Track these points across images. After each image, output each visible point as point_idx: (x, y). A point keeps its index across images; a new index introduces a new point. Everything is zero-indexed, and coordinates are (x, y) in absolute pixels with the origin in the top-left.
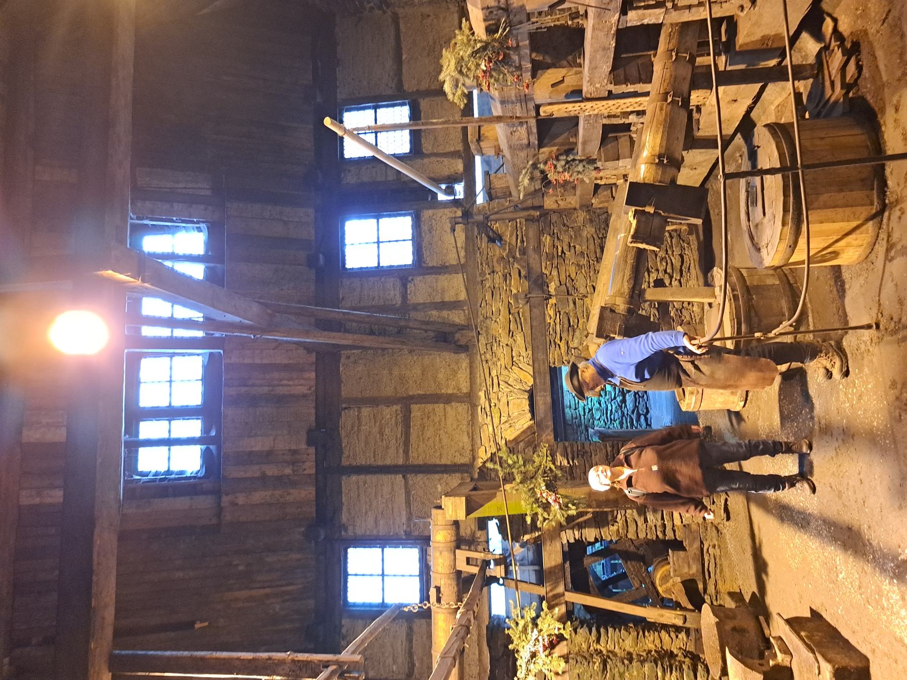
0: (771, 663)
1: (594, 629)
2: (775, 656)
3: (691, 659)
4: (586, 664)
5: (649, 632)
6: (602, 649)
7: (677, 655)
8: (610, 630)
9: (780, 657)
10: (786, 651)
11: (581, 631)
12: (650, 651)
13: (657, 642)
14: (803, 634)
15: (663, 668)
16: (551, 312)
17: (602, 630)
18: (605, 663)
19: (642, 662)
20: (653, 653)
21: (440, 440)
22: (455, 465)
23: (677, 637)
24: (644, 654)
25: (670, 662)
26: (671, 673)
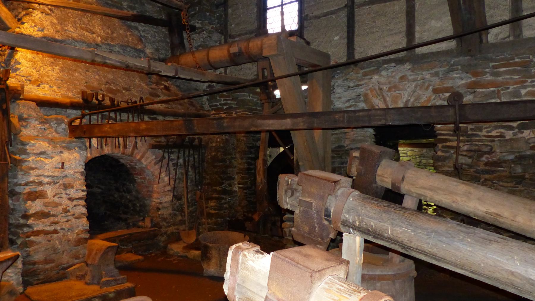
16: (494, 133)
21: (373, 33)
22: (353, 49)
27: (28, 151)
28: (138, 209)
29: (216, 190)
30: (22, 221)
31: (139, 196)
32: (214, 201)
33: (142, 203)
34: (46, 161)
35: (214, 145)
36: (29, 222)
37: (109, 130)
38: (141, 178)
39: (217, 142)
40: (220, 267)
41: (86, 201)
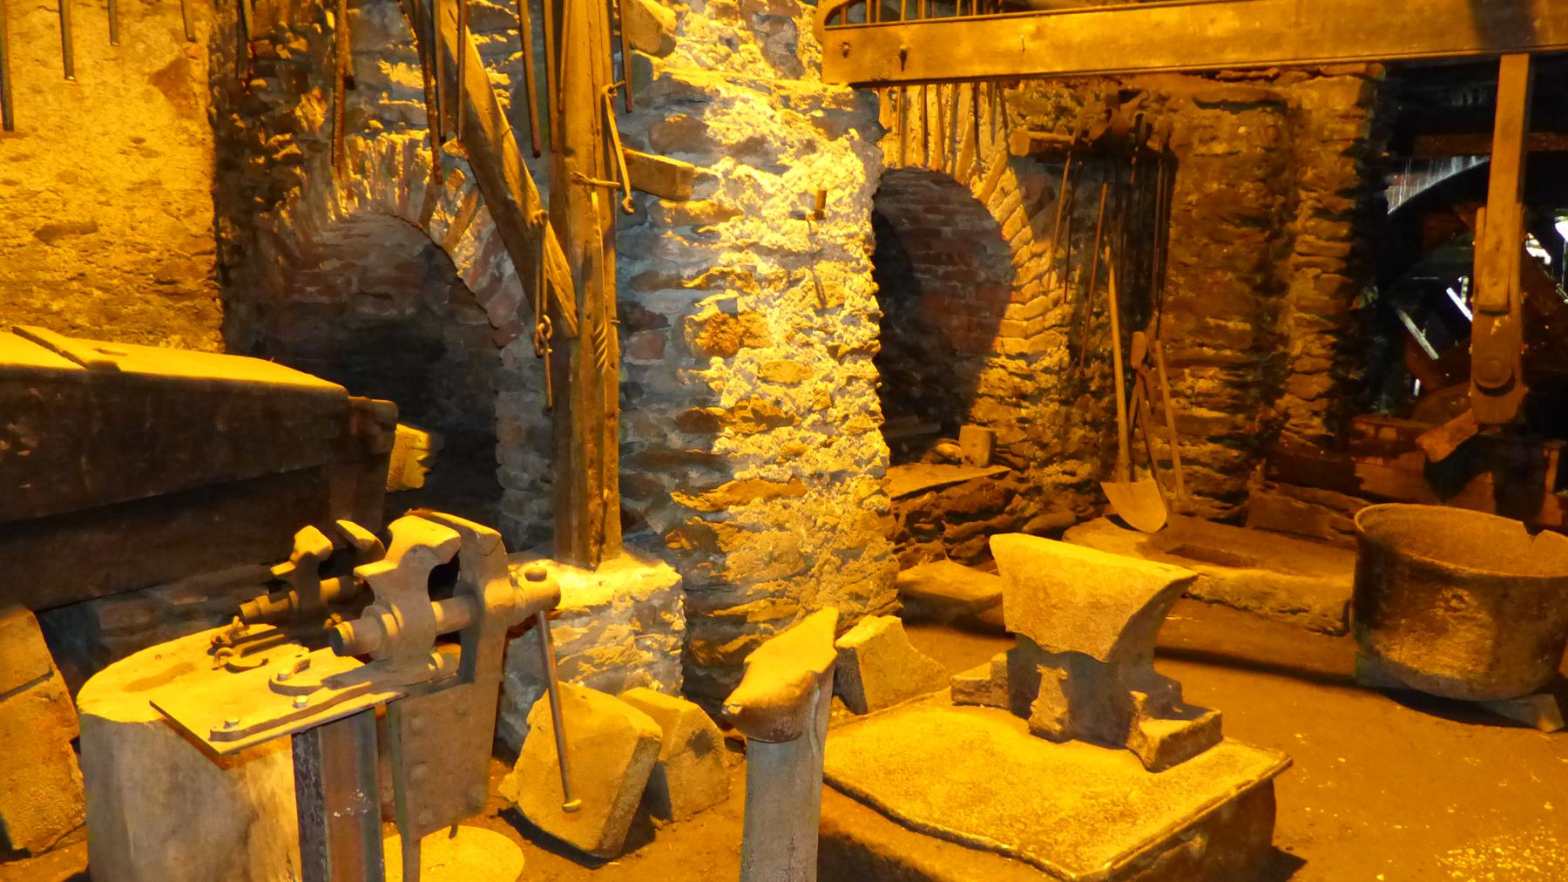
0: (1140, 696)
2: (1165, 713)
3: (1258, 436)
4: (1258, 173)
5: (1333, 345)
6: (1298, 225)
7: (1271, 404)
8: (1345, 247)
9: (1157, 729)
10: (1170, 753)
11: (1349, 169)
13: (1307, 364)
14: (1197, 843)
18: (1259, 220)
19: (1256, 318)
20: (1281, 349)
23: (1316, 414)
27: (710, 133)
28: (916, 392)
29: (1222, 331)
30: (676, 440)
31: (926, 343)
32: (1212, 372)
33: (935, 371)
34: (766, 179)
35: (1219, 148)
36: (719, 446)
37: (1031, 45)
38: (947, 277)
39: (1234, 137)
40: (1491, 667)
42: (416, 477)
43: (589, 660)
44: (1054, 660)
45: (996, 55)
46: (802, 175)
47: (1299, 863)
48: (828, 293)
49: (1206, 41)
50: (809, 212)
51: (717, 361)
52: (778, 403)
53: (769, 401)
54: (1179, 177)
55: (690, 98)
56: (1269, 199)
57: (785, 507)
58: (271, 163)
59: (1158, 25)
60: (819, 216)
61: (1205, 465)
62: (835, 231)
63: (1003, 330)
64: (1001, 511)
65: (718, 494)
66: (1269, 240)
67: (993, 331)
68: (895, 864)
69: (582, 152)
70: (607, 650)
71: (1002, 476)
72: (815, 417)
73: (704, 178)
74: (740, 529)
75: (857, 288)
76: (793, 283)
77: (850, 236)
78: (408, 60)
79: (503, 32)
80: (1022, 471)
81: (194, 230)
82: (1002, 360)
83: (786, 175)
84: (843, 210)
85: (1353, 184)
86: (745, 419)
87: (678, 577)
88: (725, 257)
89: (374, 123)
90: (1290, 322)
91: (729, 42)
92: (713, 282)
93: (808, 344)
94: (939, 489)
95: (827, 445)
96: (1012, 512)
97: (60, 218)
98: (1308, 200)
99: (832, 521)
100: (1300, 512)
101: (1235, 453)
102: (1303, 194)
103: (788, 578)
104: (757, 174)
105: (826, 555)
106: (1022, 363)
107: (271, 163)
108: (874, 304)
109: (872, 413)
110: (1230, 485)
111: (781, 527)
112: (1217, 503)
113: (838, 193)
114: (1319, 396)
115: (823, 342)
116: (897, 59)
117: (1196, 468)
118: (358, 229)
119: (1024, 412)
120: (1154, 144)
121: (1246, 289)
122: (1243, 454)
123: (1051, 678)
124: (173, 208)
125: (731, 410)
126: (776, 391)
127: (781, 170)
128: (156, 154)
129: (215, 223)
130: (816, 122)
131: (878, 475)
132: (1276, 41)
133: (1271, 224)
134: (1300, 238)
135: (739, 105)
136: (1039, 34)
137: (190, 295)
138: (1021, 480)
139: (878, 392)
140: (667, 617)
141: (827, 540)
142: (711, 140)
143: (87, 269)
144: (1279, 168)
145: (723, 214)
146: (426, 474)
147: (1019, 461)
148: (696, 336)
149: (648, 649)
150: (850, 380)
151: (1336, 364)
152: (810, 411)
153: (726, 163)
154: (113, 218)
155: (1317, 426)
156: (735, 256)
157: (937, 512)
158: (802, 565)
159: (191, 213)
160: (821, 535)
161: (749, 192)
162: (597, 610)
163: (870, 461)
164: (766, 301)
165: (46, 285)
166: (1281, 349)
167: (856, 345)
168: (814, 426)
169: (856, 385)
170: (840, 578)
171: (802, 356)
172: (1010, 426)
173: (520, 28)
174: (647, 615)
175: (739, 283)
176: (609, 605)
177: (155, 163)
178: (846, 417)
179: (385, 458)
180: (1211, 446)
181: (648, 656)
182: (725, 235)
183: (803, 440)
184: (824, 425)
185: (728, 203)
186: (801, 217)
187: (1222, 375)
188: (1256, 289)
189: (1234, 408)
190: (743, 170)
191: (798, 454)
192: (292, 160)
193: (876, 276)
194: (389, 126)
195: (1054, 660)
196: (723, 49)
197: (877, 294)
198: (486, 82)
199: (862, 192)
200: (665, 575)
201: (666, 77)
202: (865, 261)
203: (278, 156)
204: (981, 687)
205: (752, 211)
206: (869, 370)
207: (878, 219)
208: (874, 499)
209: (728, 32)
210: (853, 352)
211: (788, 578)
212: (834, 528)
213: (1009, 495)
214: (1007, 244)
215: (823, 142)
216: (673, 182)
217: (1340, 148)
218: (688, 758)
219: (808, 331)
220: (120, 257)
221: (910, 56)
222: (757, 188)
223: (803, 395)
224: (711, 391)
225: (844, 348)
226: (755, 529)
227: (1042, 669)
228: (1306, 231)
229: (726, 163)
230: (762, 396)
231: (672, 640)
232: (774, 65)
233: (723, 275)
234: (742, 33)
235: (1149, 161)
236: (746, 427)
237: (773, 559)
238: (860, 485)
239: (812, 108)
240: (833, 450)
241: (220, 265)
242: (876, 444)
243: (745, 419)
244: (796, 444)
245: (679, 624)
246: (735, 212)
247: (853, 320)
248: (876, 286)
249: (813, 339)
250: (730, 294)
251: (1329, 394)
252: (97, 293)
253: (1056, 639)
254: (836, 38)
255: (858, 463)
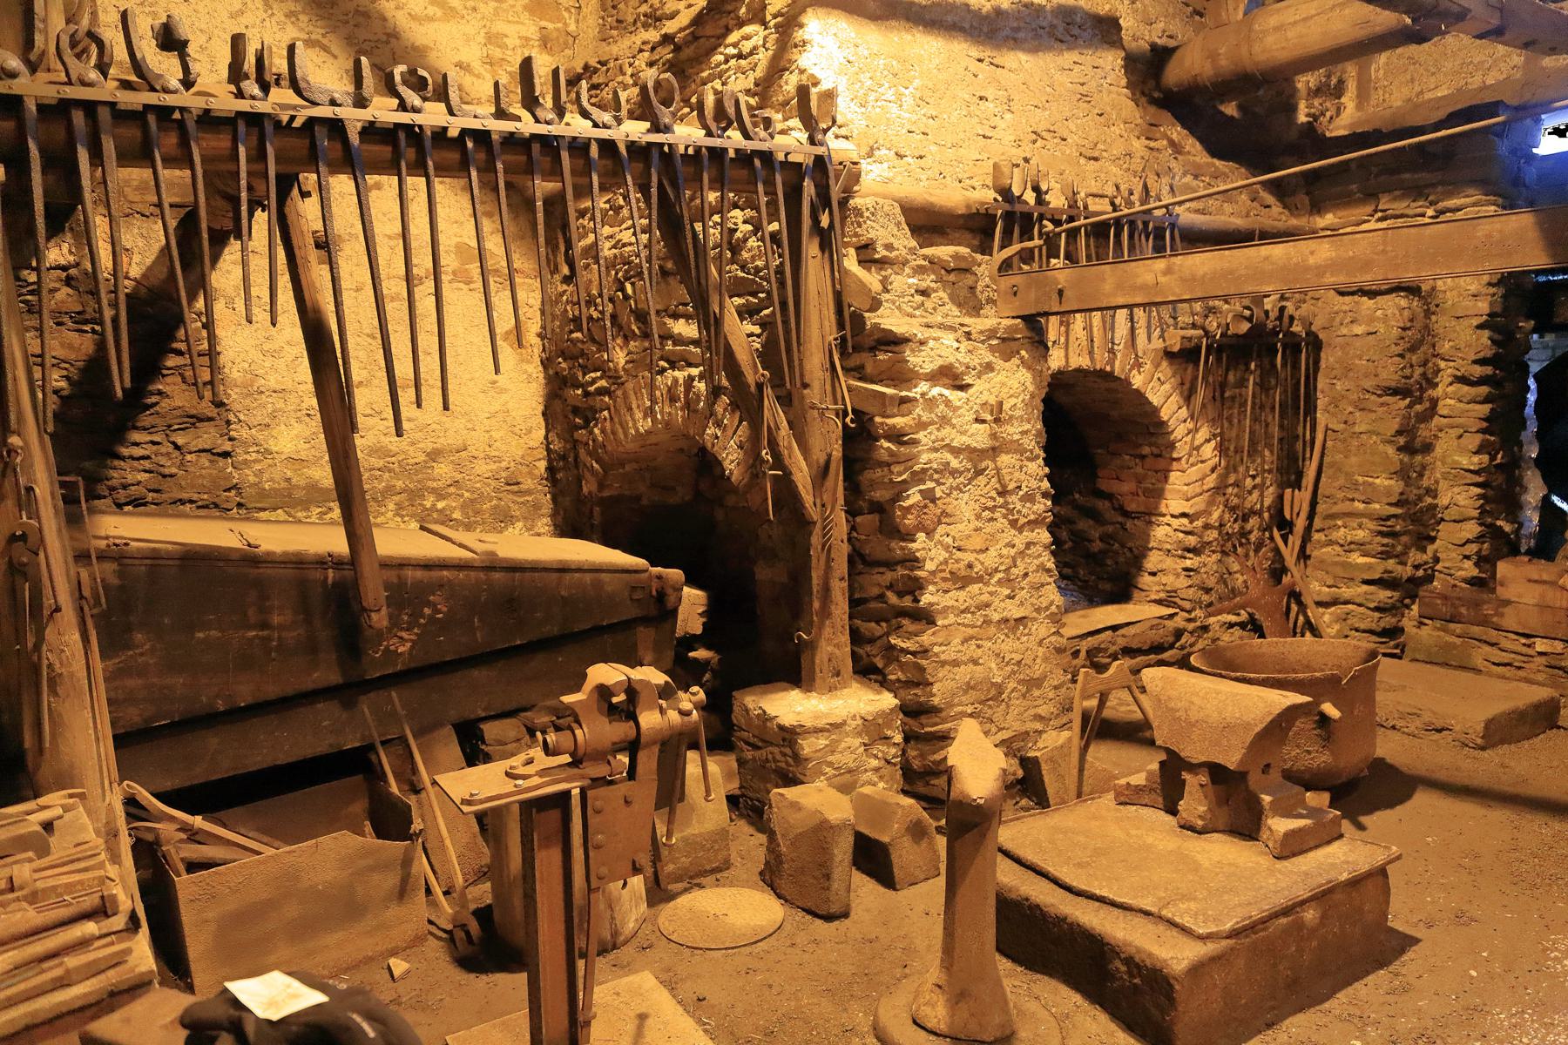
0: (1267, 798)
1: (1489, 370)
4: (1398, 350)
5: (1480, 496)
7: (1424, 550)
9: (1280, 825)
10: (1291, 847)
12: (1433, 492)
13: (1453, 513)
14: (1310, 915)
15: (1388, 518)
17: (1484, 390)
19: (1402, 473)
20: (1429, 500)
23: (1467, 557)
24: (1425, 483)
25: (1405, 533)
26: (1381, 533)
33: (1110, 529)
34: (955, 396)
37: (1162, 279)
41: (1052, 529)
42: (696, 627)
43: (830, 764)
44: (1193, 768)
45: (1135, 289)
46: (983, 390)
47: (1416, 941)
48: (1007, 478)
49: (1307, 269)
50: (989, 418)
51: (921, 536)
52: (970, 566)
53: (962, 565)
54: (1323, 355)
55: (893, 342)
56: (1408, 372)
57: (979, 647)
58: (587, 394)
59: (1267, 258)
60: (997, 420)
61: (1360, 605)
62: (1011, 430)
63: (1167, 495)
64: (1172, 646)
65: (926, 639)
66: (1410, 406)
67: (1158, 494)
68: (1061, 920)
69: (816, 385)
70: (844, 759)
71: (1171, 616)
72: (1001, 575)
73: (904, 401)
74: (943, 663)
75: (1032, 473)
76: (979, 473)
77: (1023, 433)
78: (688, 317)
79: (754, 294)
80: (1189, 612)
81: (532, 444)
82: (1168, 519)
83: (971, 391)
84: (1018, 413)
85: (1489, 353)
86: (944, 580)
87: (897, 701)
88: (924, 458)
89: (662, 363)
90: (1436, 473)
91: (924, 293)
92: (919, 477)
93: (992, 519)
94: (1115, 628)
95: (1011, 597)
96: (1182, 648)
97: (442, 442)
98: (1447, 371)
99: (1017, 657)
100: (1454, 646)
101: (1389, 593)
102: (1442, 364)
103: (982, 702)
104: (946, 392)
105: (1012, 685)
106: (1185, 521)
107: (587, 394)
108: (1046, 484)
109: (1048, 571)
110: (1388, 621)
111: (975, 662)
112: (1374, 638)
113: (1013, 401)
114: (1468, 541)
115: (1005, 516)
116: (1055, 296)
117: (1350, 606)
118: (653, 439)
119: (1188, 563)
120: (1297, 328)
121: (1391, 450)
122: (1396, 595)
123: (1192, 781)
124: (516, 430)
125: (933, 573)
126: (968, 557)
127: (963, 388)
128: (505, 391)
129: (546, 437)
130: (992, 349)
131: (1056, 619)
132: (1367, 265)
133: (1414, 391)
134: (1441, 403)
135: (931, 343)
136: (1168, 271)
137: (529, 492)
138: (1189, 620)
139: (1053, 553)
140: (889, 733)
141: (1013, 672)
142: (912, 371)
143: (459, 477)
144: (1419, 339)
145: (922, 426)
146: (704, 624)
147: (1187, 605)
148: (904, 517)
149: (876, 757)
150: (1028, 545)
151: (1483, 512)
152: (996, 570)
153: (924, 386)
154: (477, 442)
155: (1470, 569)
156: (933, 456)
157: (1113, 649)
158: (993, 692)
159: (529, 431)
160: (1009, 669)
161: (942, 407)
162: (836, 726)
163: (1047, 608)
164: (958, 488)
165: (434, 491)
166: (1429, 500)
167: (1032, 517)
168: (999, 581)
169: (1033, 550)
170: (1025, 703)
171: (989, 528)
172: (1178, 575)
173: (769, 293)
174: (873, 730)
175: (936, 476)
176: (844, 723)
177: (504, 397)
178: (1026, 575)
179: (674, 612)
180: (1365, 588)
181: (875, 763)
182: (924, 441)
183: (991, 594)
184: (1007, 581)
185: (925, 417)
186: (984, 421)
187: (1372, 525)
188: (1399, 449)
189: (1385, 555)
190: (936, 391)
191: (988, 605)
192: (602, 392)
193: (1047, 462)
194: (673, 366)
195: (1193, 768)
196: (918, 298)
197: (1049, 477)
198: (742, 335)
199: (1032, 396)
200: (888, 700)
201: (876, 326)
202: (1037, 451)
203: (592, 389)
204: (1138, 789)
205: (944, 421)
206: (1045, 537)
207: (1046, 419)
208: (1053, 638)
209: (924, 285)
210: (1029, 522)
211: (982, 702)
212: (1019, 662)
213: (1179, 633)
214: (1163, 424)
215: (999, 363)
216: (884, 405)
217: (1475, 322)
218: (907, 842)
219: (992, 509)
220: (482, 468)
221: (1067, 293)
222: (948, 403)
223: (990, 559)
224: (917, 560)
225: (1022, 521)
226: (956, 663)
227: (1185, 775)
228: (1446, 396)
229: (924, 386)
230: (957, 561)
231: (893, 751)
232: (959, 305)
233: (924, 471)
234: (933, 285)
235: (1293, 346)
236: (945, 586)
237: (969, 687)
238: (1041, 629)
239: (989, 338)
240: (1017, 601)
241: (550, 469)
242: (1052, 595)
243: (944, 580)
244: (985, 598)
245: (898, 738)
246: (931, 423)
247: (1029, 498)
248: (1047, 470)
249: (997, 515)
250: (930, 485)
251: (1479, 539)
252: (467, 495)
253: (1194, 752)
254: (1006, 282)
255: (1038, 610)
